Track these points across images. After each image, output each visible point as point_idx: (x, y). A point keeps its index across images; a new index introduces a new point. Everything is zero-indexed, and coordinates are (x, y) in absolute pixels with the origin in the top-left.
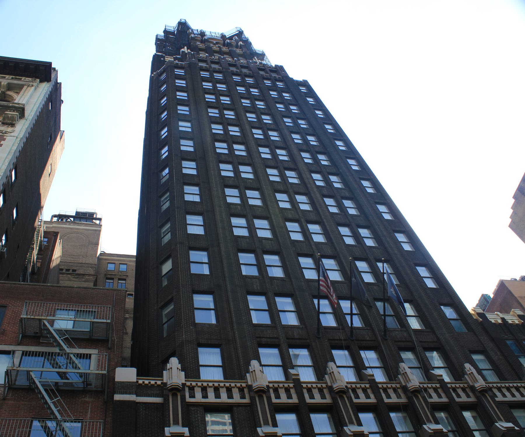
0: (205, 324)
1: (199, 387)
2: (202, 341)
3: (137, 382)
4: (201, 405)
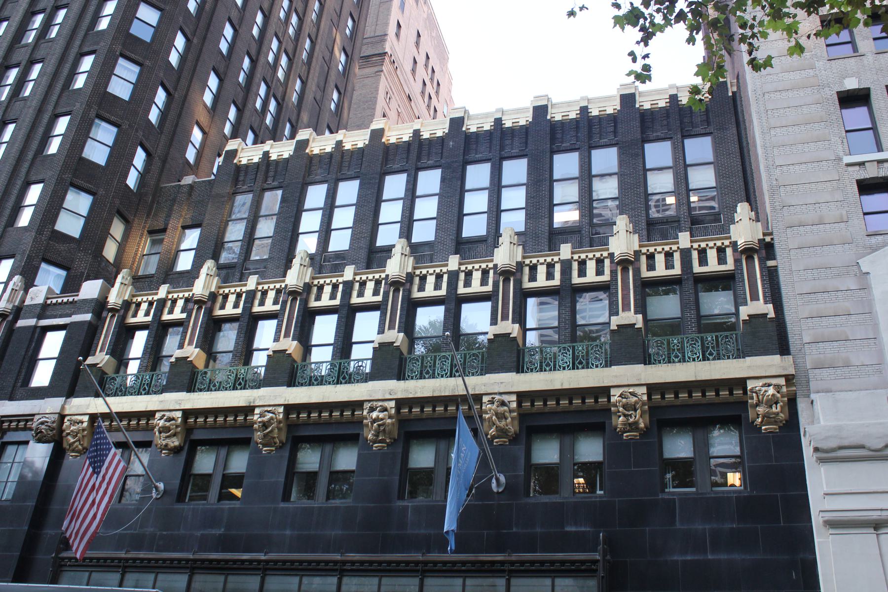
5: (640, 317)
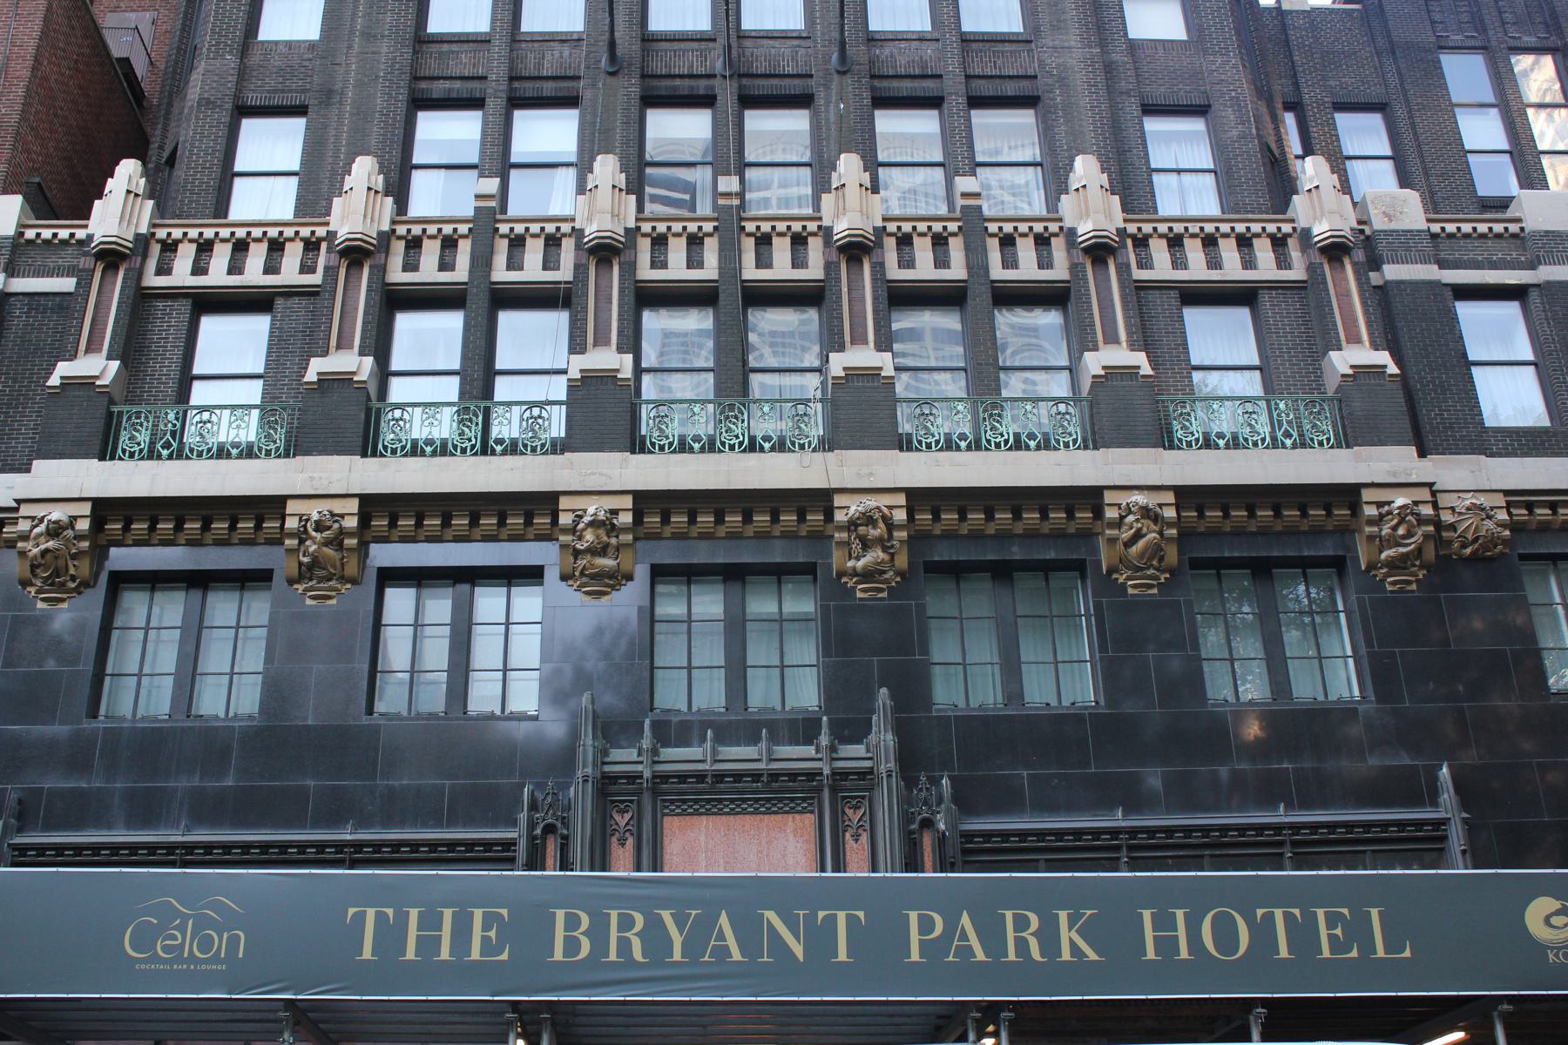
0: (276, 43)
1: (224, 241)
2: (253, 99)
3: (22, 234)
4: (186, 296)
5: (629, 358)
